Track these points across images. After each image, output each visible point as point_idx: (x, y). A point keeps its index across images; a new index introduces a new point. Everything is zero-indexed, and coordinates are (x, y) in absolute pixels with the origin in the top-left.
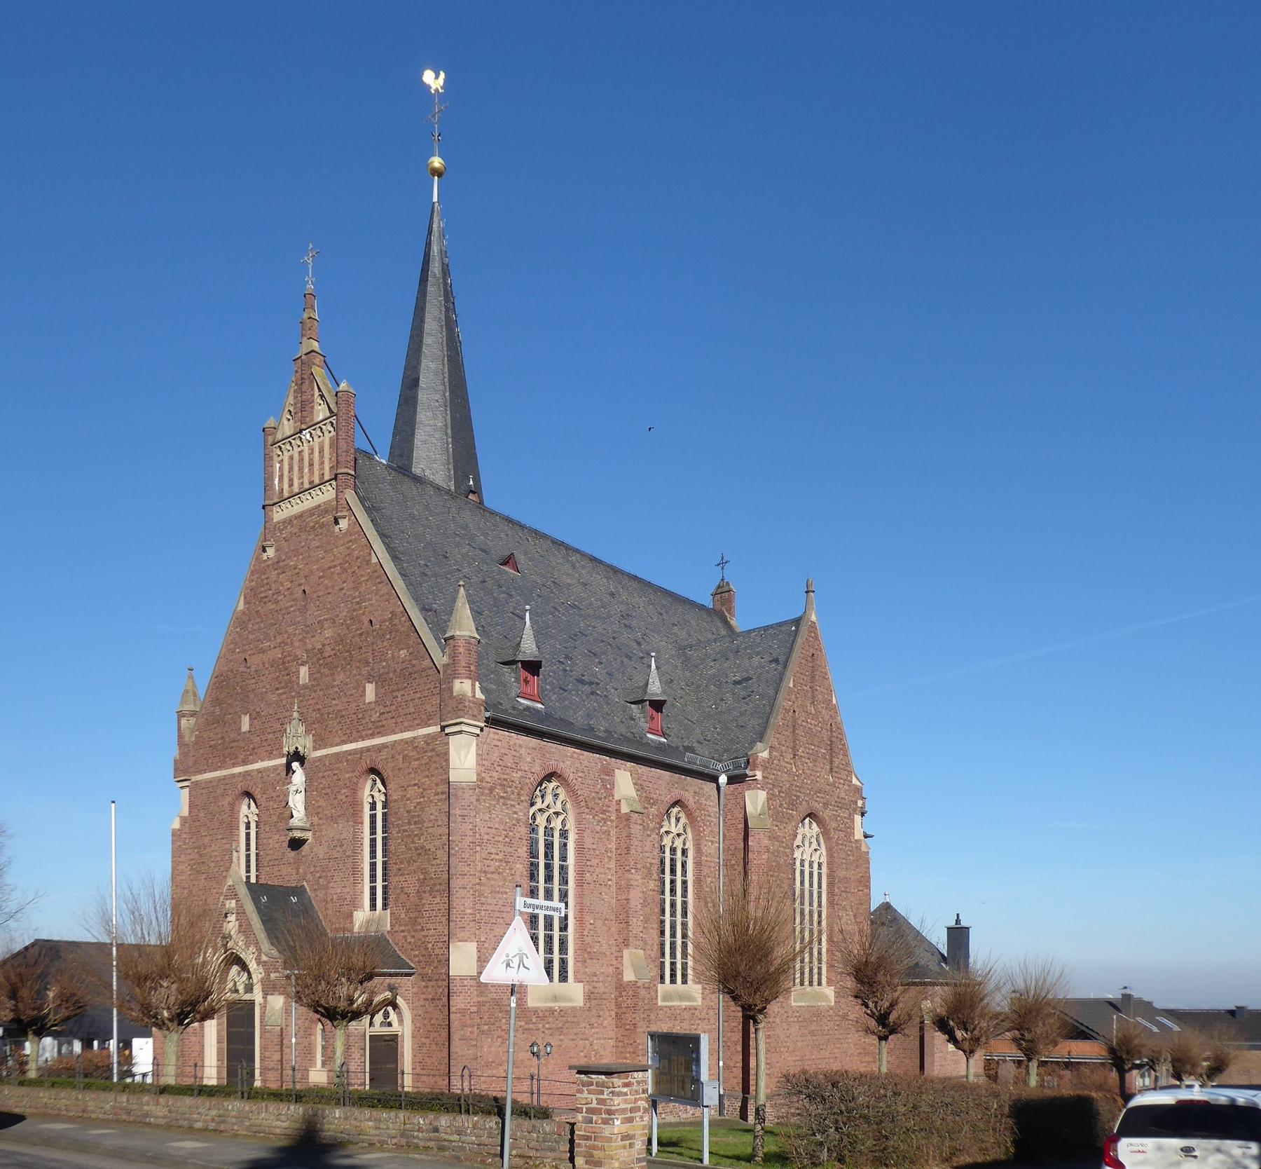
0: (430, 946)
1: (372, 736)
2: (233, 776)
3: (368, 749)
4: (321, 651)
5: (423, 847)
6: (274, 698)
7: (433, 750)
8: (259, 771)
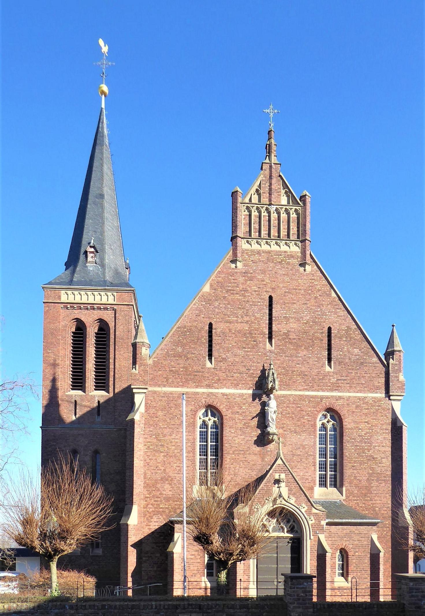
0: (377, 509)
1: (332, 390)
2: (197, 393)
3: (327, 397)
4: (287, 334)
5: (371, 456)
6: (241, 352)
7: (379, 406)
8: (223, 394)
